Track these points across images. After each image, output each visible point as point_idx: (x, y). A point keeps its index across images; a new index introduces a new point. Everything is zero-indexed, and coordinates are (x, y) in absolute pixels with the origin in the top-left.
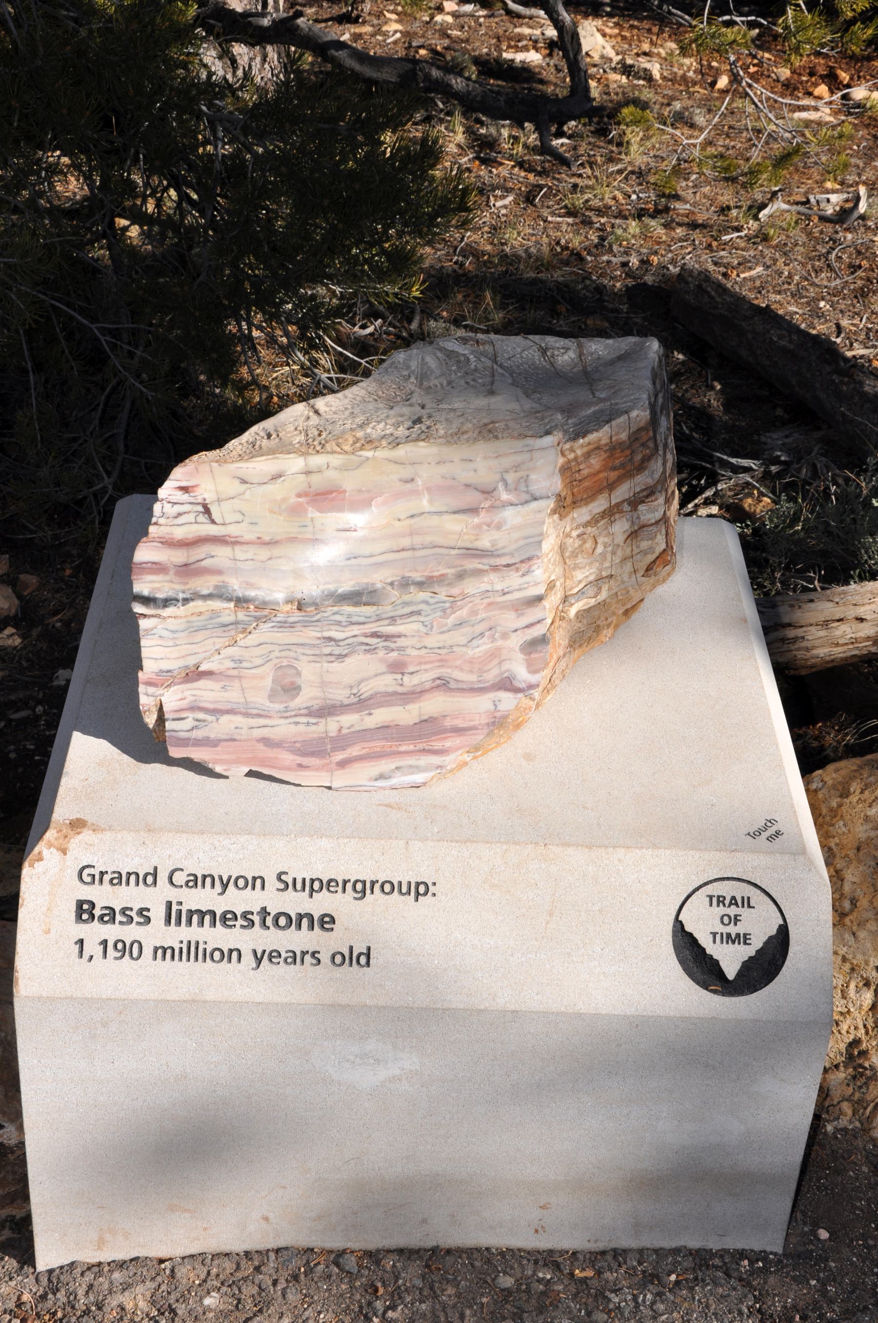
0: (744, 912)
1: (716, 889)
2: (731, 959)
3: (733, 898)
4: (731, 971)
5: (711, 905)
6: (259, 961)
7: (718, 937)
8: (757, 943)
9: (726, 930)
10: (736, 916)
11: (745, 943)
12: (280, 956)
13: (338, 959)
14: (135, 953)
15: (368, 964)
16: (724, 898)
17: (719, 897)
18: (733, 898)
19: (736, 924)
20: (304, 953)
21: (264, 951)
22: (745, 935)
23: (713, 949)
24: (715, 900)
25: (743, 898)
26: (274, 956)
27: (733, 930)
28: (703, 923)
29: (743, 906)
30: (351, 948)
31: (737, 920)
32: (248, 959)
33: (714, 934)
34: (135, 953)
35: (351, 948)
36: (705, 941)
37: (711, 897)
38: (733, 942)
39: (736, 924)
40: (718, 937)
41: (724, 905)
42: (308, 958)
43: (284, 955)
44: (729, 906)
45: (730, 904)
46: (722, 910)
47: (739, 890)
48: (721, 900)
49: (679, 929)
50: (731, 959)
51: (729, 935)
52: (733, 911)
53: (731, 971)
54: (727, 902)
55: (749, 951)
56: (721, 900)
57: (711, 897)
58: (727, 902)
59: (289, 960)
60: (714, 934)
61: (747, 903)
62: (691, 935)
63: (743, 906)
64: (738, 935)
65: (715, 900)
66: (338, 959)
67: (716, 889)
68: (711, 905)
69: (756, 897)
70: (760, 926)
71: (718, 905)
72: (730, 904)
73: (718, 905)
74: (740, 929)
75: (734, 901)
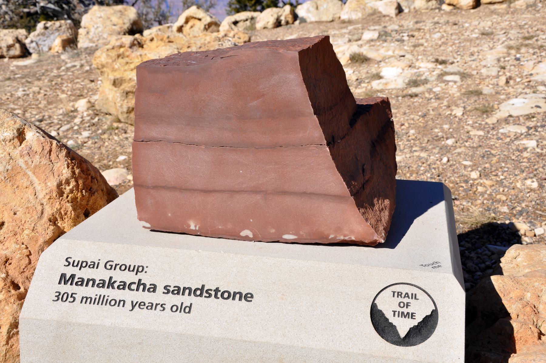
1: (397, 288)
2: (403, 327)
3: (407, 294)
5: (394, 296)
6: (133, 307)
7: (397, 313)
8: (419, 318)
9: (401, 310)
10: (407, 303)
11: (412, 318)
12: (144, 305)
13: (174, 309)
14: (64, 299)
15: (189, 312)
16: (402, 293)
17: (398, 293)
18: (407, 294)
19: (407, 308)
20: (157, 305)
21: (137, 303)
22: (412, 314)
24: (396, 294)
25: (412, 294)
26: (141, 304)
27: (405, 310)
28: (388, 306)
29: (412, 298)
30: (182, 303)
31: (408, 305)
32: (128, 306)
33: (394, 312)
34: (64, 299)
35: (182, 303)
36: (389, 315)
37: (394, 292)
38: (405, 317)
39: (407, 308)
40: (397, 313)
41: (401, 297)
42: (159, 307)
43: (147, 305)
44: (404, 297)
45: (404, 297)
46: (400, 299)
47: (410, 290)
48: (399, 294)
50: (403, 327)
51: (403, 313)
52: (406, 300)
54: (403, 296)
55: (415, 323)
57: (394, 292)
58: (403, 296)
59: (149, 308)
60: (394, 312)
63: (412, 298)
64: (408, 313)
65: (396, 294)
66: (174, 309)
67: (397, 288)
68: (394, 296)
71: (398, 297)
73: (398, 297)
74: (410, 310)
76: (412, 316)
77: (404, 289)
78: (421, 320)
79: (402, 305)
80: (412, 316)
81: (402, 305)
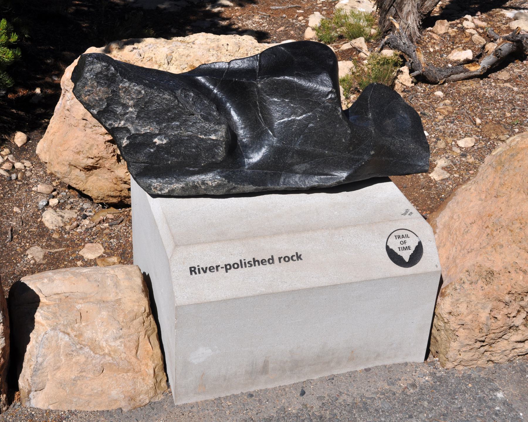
0: (407, 239)
1: (396, 233)
2: (406, 256)
4: (407, 259)
9: (402, 246)
23: (399, 253)
27: (405, 246)
28: (395, 245)
33: (399, 248)
46: (400, 240)
47: (404, 233)
49: (387, 247)
50: (406, 256)
51: (404, 248)
52: (403, 239)
53: (407, 259)
55: (411, 252)
56: (399, 237)
60: (399, 248)
61: (407, 236)
64: (406, 247)
70: (413, 244)
74: (407, 245)
75: (403, 237)
76: (409, 248)
77: (400, 233)
80: (409, 248)
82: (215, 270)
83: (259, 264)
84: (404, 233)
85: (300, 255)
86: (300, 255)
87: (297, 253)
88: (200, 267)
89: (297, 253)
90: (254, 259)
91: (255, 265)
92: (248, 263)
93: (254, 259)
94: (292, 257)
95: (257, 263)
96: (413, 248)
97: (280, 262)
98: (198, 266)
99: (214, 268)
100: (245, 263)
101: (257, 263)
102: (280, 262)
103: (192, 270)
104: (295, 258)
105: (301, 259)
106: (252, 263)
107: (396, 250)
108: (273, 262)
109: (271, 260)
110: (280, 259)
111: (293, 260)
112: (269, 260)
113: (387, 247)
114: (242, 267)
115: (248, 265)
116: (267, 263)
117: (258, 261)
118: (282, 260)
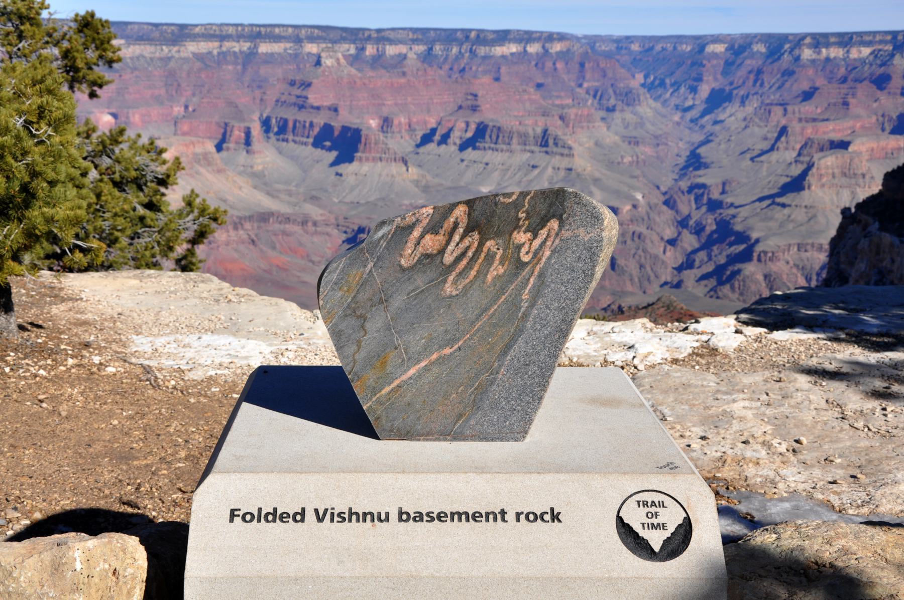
0: (660, 510)
3: (653, 502)
7: (646, 526)
9: (650, 521)
10: (656, 513)
18: (653, 502)
23: (643, 533)
24: (641, 504)
27: (655, 521)
28: (635, 518)
31: (656, 515)
33: (643, 524)
37: (639, 502)
40: (646, 526)
45: (652, 506)
46: (647, 510)
47: (657, 497)
48: (645, 504)
51: (653, 524)
54: (649, 504)
56: (645, 504)
57: (639, 502)
58: (649, 504)
60: (643, 524)
61: (662, 505)
62: (628, 525)
64: (658, 524)
65: (641, 504)
69: (668, 501)
70: (672, 518)
72: (652, 506)
74: (660, 520)
76: (663, 526)
77: (649, 497)
78: (673, 530)
79: (650, 515)
80: (663, 526)
81: (650, 515)
82: (484, 519)
83: (468, 520)
84: (657, 497)
85: (559, 513)
86: (559, 513)
87: (552, 510)
88: (336, 512)
89: (552, 510)
90: (350, 509)
91: (350, 520)
92: (339, 515)
93: (350, 509)
94: (542, 515)
95: (354, 517)
96: (671, 529)
97: (518, 520)
98: (333, 509)
99: (446, 516)
100: (332, 514)
101: (354, 517)
102: (518, 520)
103: (233, 514)
104: (547, 517)
105: (559, 521)
106: (346, 516)
107: (637, 528)
108: (302, 520)
109: (300, 516)
110: (518, 515)
111: (543, 519)
112: (296, 514)
113: (620, 519)
114: (259, 521)
115: (336, 519)
116: (291, 520)
117: (357, 514)
118: (522, 517)
